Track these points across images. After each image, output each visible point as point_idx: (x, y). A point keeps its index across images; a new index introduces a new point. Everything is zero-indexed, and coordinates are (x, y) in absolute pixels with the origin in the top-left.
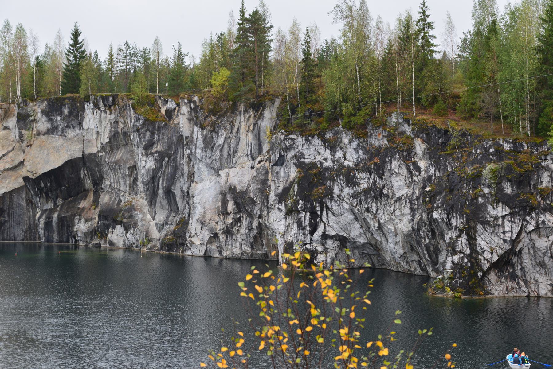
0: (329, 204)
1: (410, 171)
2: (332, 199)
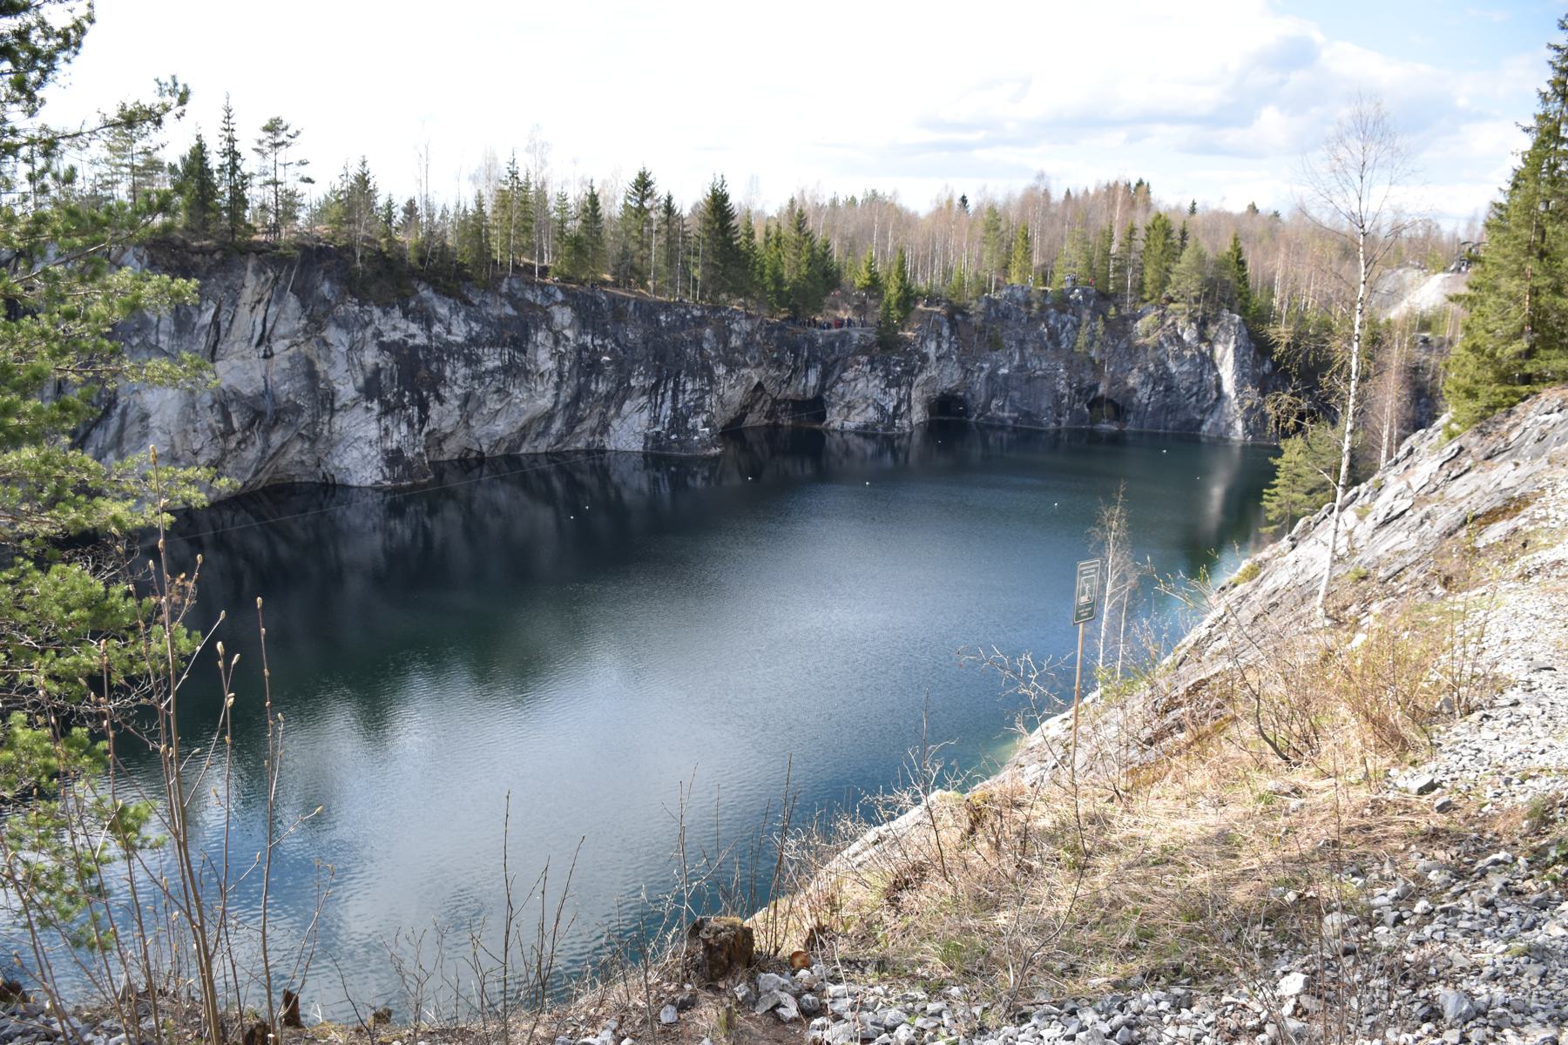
0: (442, 391)
1: (557, 342)
2: (445, 385)
